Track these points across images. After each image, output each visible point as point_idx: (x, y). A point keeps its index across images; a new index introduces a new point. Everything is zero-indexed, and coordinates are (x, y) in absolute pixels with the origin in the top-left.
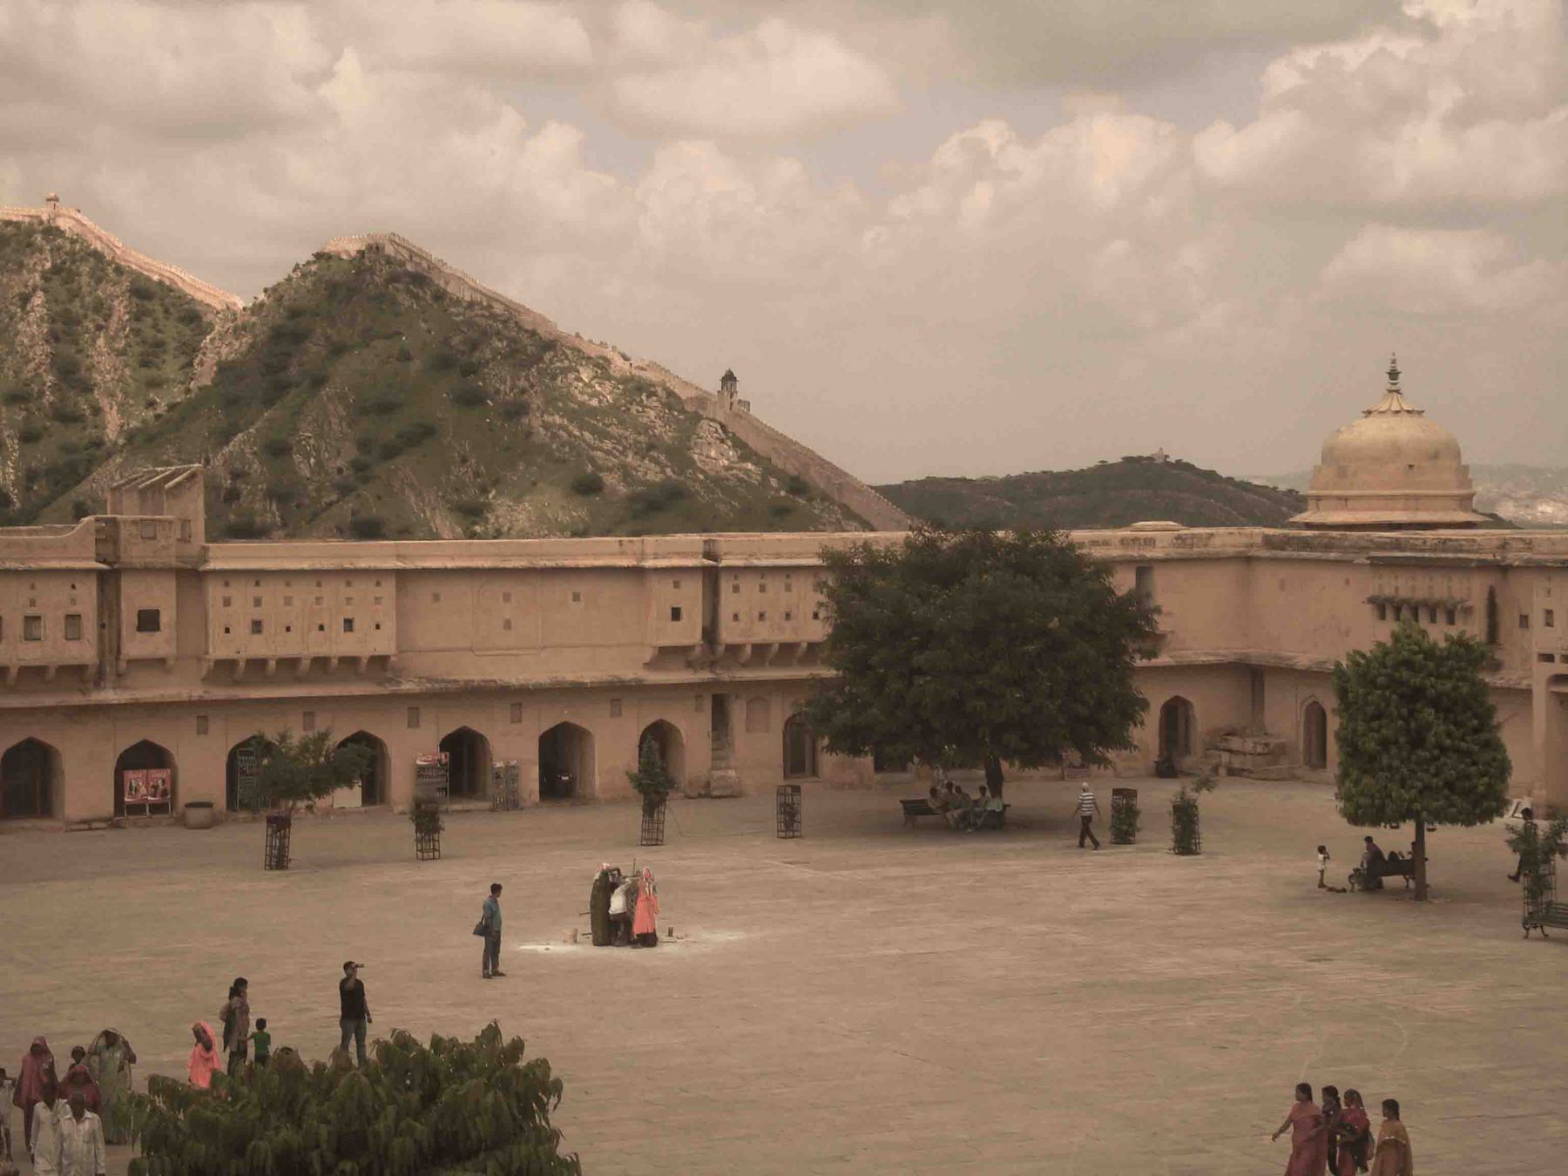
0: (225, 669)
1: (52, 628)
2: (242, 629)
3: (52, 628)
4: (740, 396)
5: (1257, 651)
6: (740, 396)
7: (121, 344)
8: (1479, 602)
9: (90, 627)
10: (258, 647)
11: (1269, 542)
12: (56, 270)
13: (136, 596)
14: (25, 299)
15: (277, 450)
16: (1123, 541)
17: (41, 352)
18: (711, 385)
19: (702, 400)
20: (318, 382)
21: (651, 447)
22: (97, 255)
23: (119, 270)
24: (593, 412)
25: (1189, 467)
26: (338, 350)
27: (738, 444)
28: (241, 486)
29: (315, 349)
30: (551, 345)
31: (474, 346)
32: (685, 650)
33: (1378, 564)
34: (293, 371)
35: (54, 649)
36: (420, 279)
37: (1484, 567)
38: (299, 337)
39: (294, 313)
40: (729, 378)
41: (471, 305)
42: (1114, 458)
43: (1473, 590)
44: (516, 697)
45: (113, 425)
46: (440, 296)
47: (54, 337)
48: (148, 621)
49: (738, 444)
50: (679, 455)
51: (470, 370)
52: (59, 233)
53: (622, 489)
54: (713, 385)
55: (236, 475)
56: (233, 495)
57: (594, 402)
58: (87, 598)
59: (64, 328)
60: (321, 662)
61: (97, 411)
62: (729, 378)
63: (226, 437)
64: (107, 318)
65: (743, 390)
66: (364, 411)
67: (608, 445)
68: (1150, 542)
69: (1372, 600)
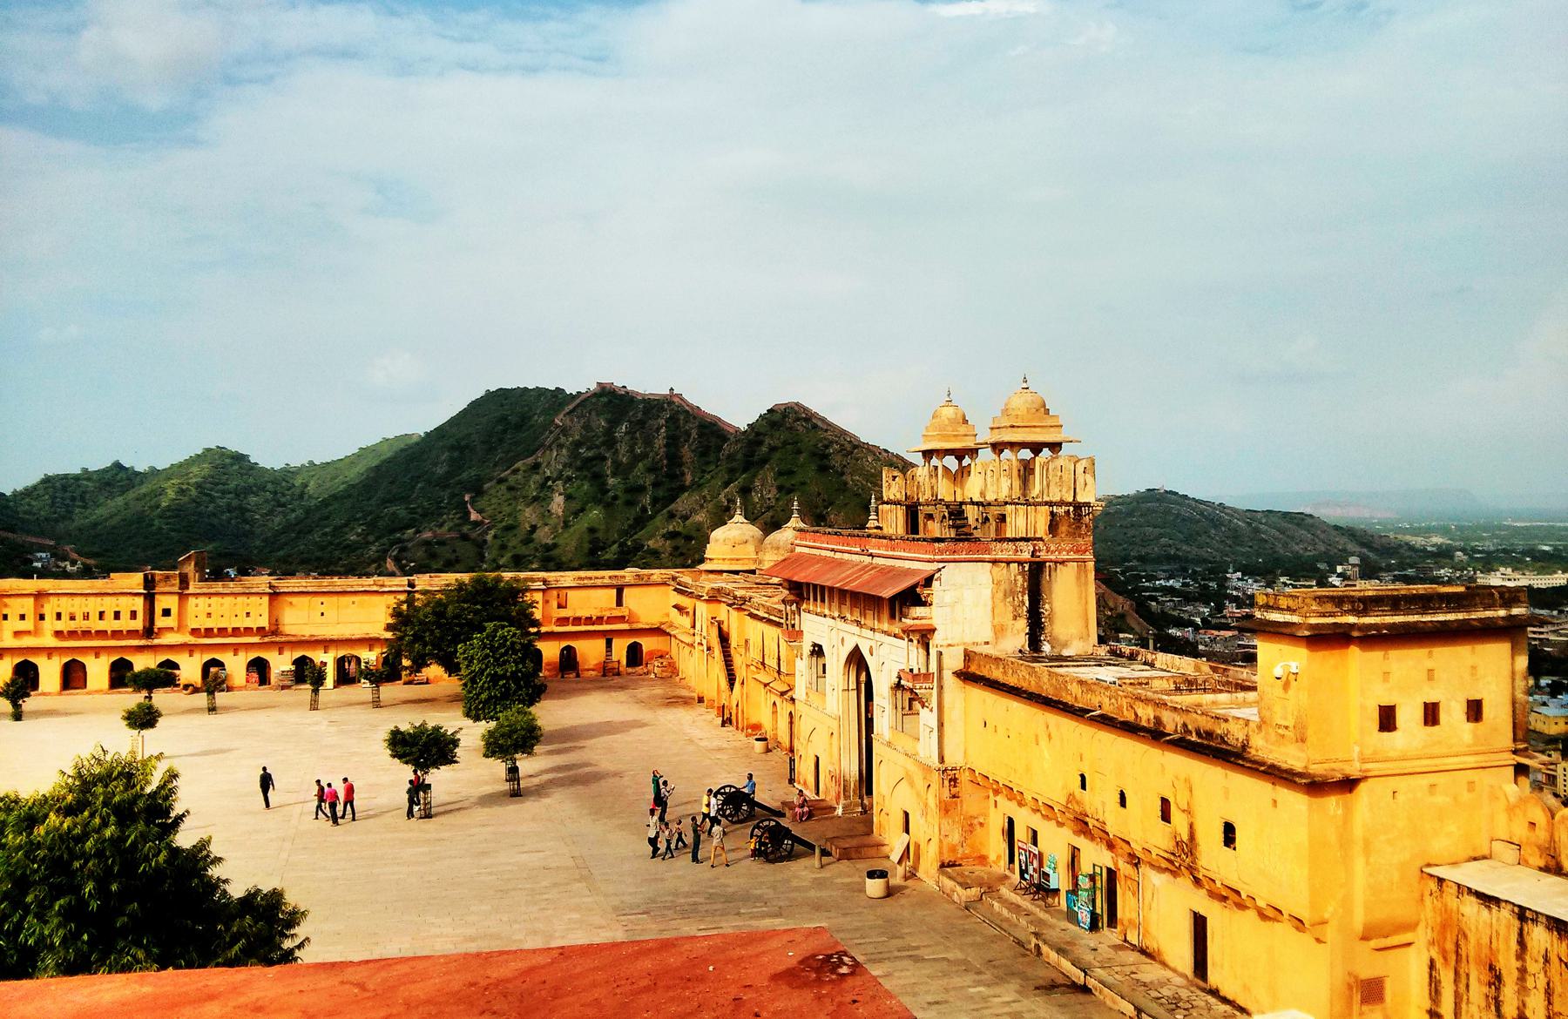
0: (195, 632)
1: (125, 615)
2: (203, 617)
3: (125, 615)
9: (140, 615)
10: (209, 624)
13: (162, 603)
14: (658, 429)
20: (764, 461)
30: (855, 447)
31: (827, 447)
35: (125, 624)
39: (758, 434)
44: (326, 644)
48: (167, 613)
58: (139, 604)
59: (673, 442)
60: (236, 632)
61: (683, 474)
63: (726, 484)
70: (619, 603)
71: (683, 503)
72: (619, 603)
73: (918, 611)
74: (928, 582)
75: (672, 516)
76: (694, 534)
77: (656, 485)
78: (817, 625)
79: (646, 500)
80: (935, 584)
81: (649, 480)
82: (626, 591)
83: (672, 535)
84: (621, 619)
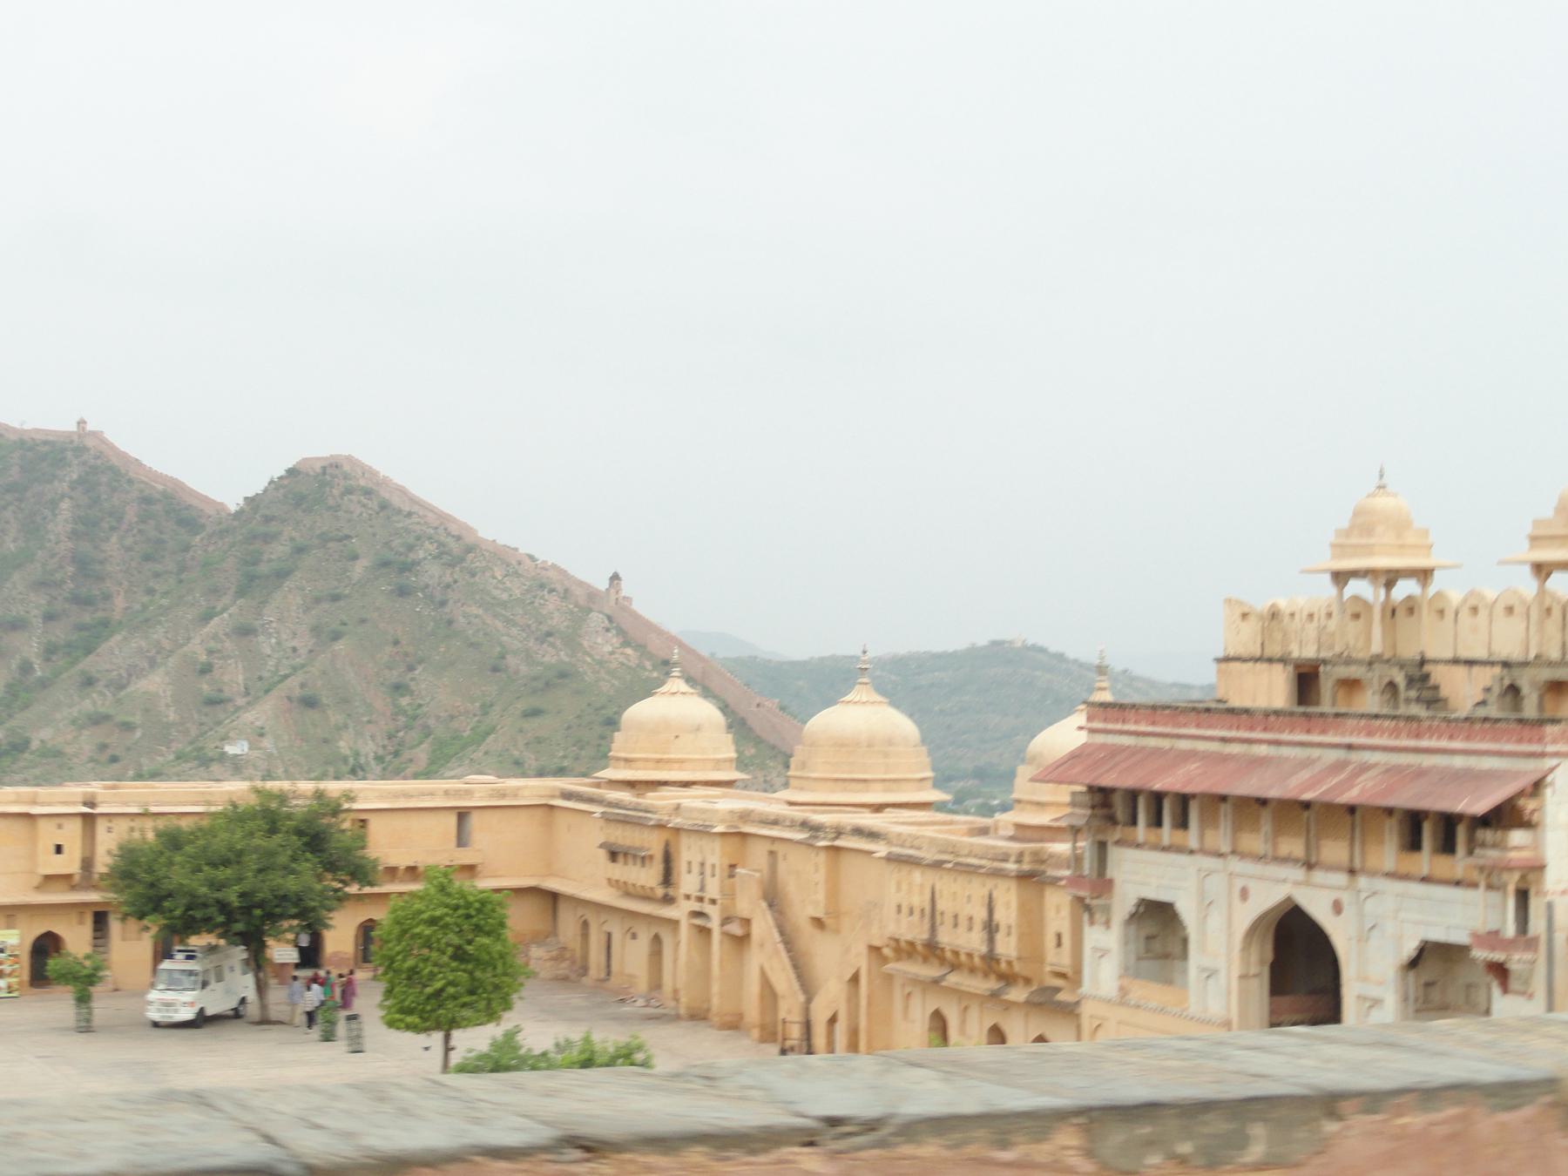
4: (623, 593)
5: (552, 884)
6: (623, 593)
7: (129, 541)
8: (657, 851)
11: (568, 796)
12: (81, 481)
14: (54, 504)
15: (245, 631)
16: (447, 793)
17: (65, 546)
18: (602, 584)
19: (593, 595)
20: (282, 575)
21: (549, 634)
22: (111, 468)
23: (130, 481)
24: (504, 605)
25: (1043, 650)
26: (300, 550)
27: (621, 632)
28: (217, 663)
29: (280, 549)
30: (470, 549)
31: (411, 548)
32: (68, 877)
33: (608, 819)
34: (263, 568)
36: (368, 493)
37: (661, 826)
38: (268, 538)
39: (268, 520)
40: (615, 577)
41: (410, 514)
42: (982, 641)
43: (653, 843)
45: (117, 615)
46: (384, 506)
47: (75, 535)
49: (621, 632)
50: (572, 641)
51: (407, 568)
52: (85, 449)
53: (524, 669)
54: (602, 584)
55: (210, 652)
56: (206, 670)
57: (505, 596)
61: (107, 597)
62: (615, 577)
63: (206, 618)
64: (120, 519)
65: (626, 589)
66: (318, 601)
67: (514, 631)
68: (469, 793)
69: (601, 846)
70: (462, 840)
71: (115, 653)
72: (462, 840)
73: (1517, 837)
74: (1537, 787)
75: (89, 682)
76: (137, 719)
77: (49, 617)
78: (1142, 871)
79: (30, 646)
80: (1548, 792)
81: (37, 604)
82: (475, 820)
83: (97, 720)
84: (470, 869)
